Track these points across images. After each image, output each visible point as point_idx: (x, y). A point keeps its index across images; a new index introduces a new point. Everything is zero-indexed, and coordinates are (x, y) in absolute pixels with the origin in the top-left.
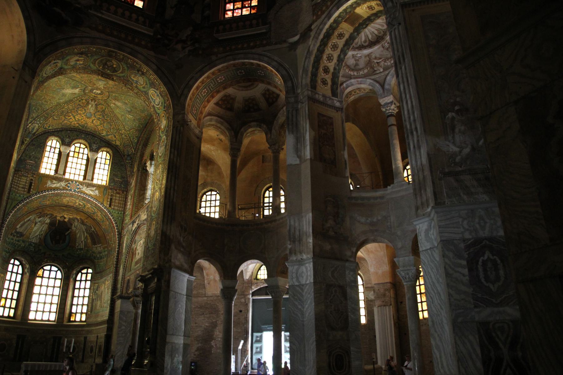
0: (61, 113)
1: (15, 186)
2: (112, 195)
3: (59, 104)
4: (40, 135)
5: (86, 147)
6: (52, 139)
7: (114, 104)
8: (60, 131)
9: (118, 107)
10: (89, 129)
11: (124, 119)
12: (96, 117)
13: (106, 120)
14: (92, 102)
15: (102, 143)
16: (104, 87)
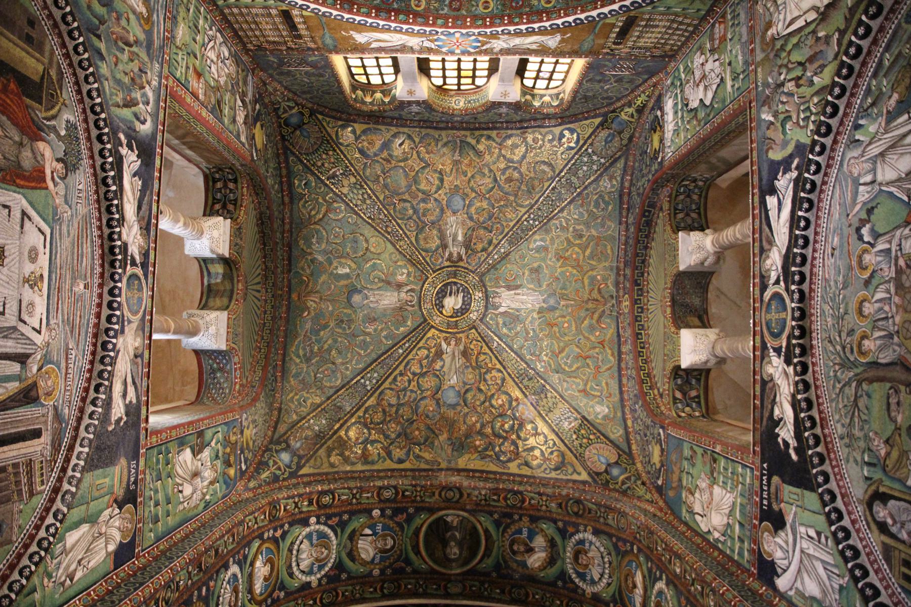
0: (533, 189)
1: (684, 27)
2: (300, 37)
3: (545, 224)
4: (587, 112)
5: (439, 87)
6: (547, 99)
7: (399, 286)
8: (530, 120)
9: (389, 283)
10: (445, 140)
11: (356, 242)
12: (436, 200)
13: (405, 201)
14: (459, 253)
15: (397, 115)
16: (442, 353)
